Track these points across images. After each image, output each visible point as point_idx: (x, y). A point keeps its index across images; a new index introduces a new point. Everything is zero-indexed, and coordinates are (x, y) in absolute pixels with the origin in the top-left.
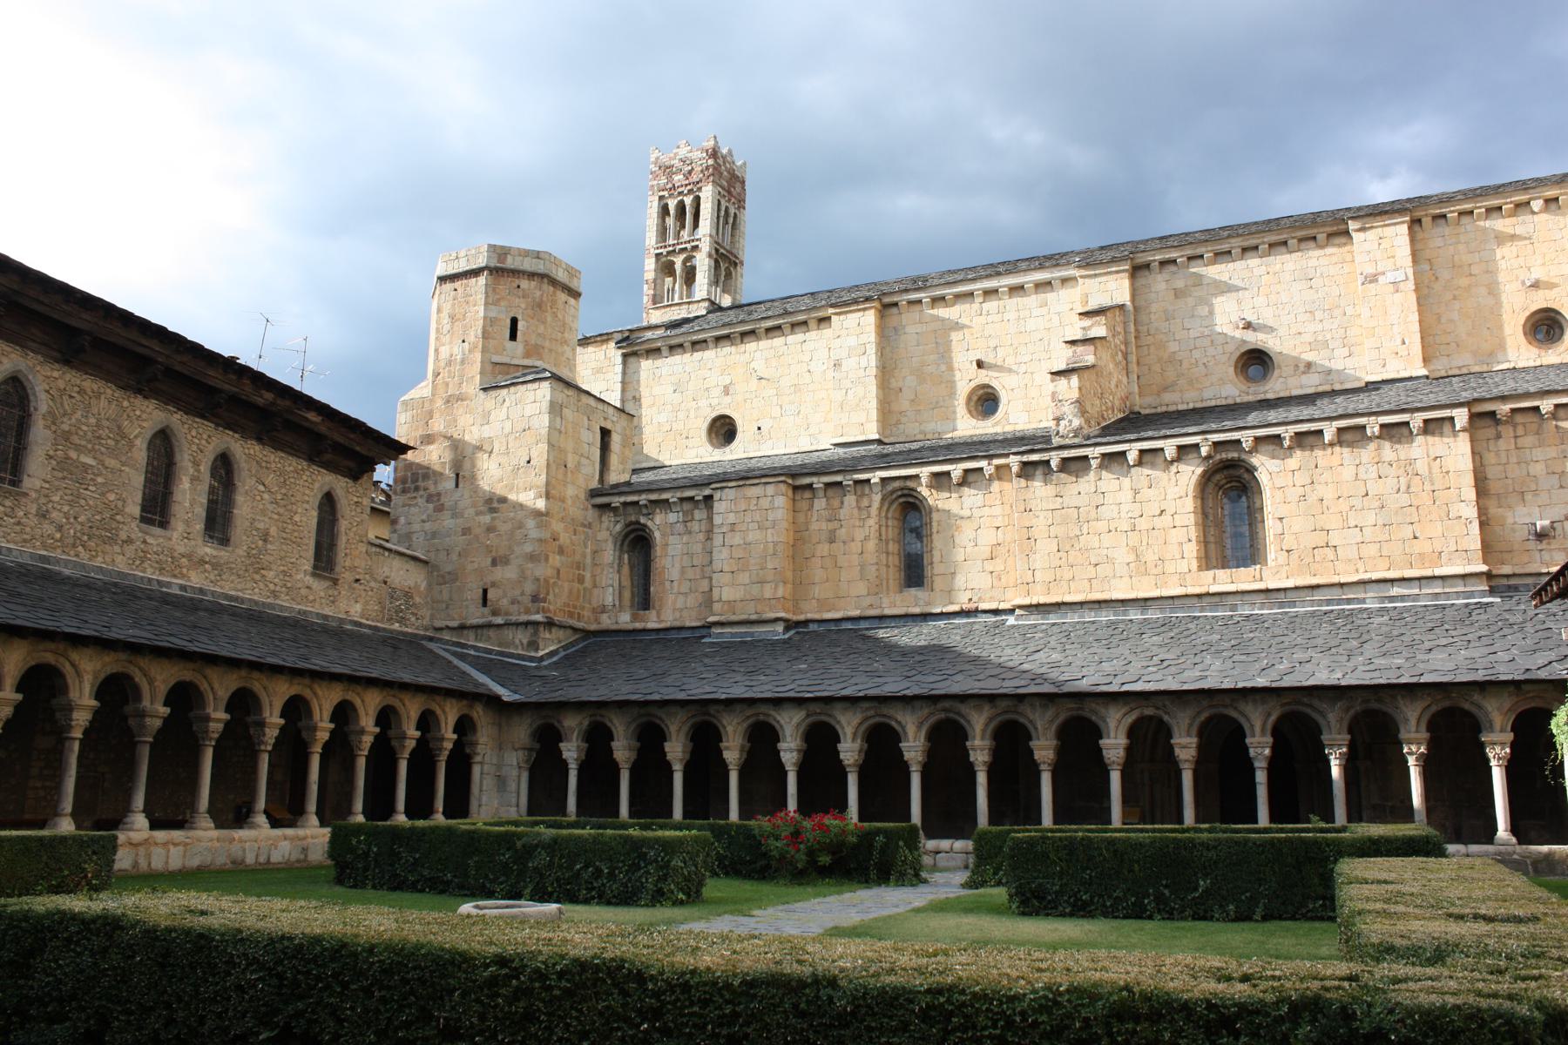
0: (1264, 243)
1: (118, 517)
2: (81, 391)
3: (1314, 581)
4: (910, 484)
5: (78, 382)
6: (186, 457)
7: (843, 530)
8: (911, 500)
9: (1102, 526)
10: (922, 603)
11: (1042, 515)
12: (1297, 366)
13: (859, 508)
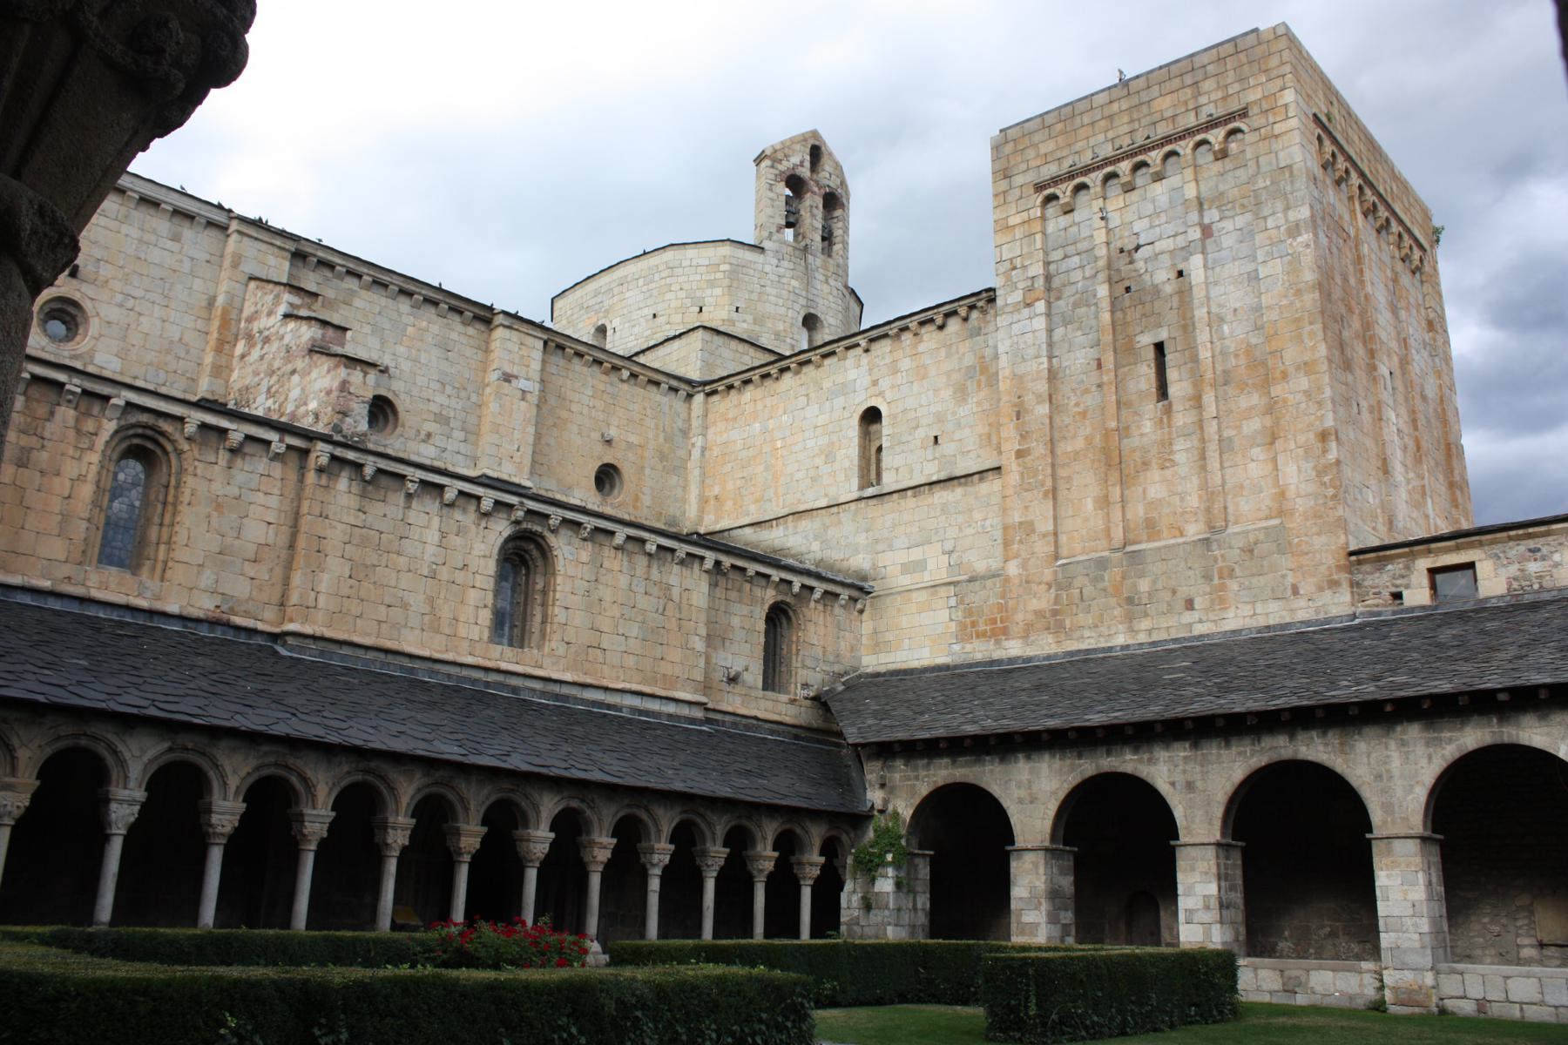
0: (419, 294)
3: (589, 680)
4: (166, 426)
7: (44, 455)
8: (150, 445)
9: (402, 561)
10: (148, 594)
11: (340, 527)
12: (418, 431)
13: (78, 431)
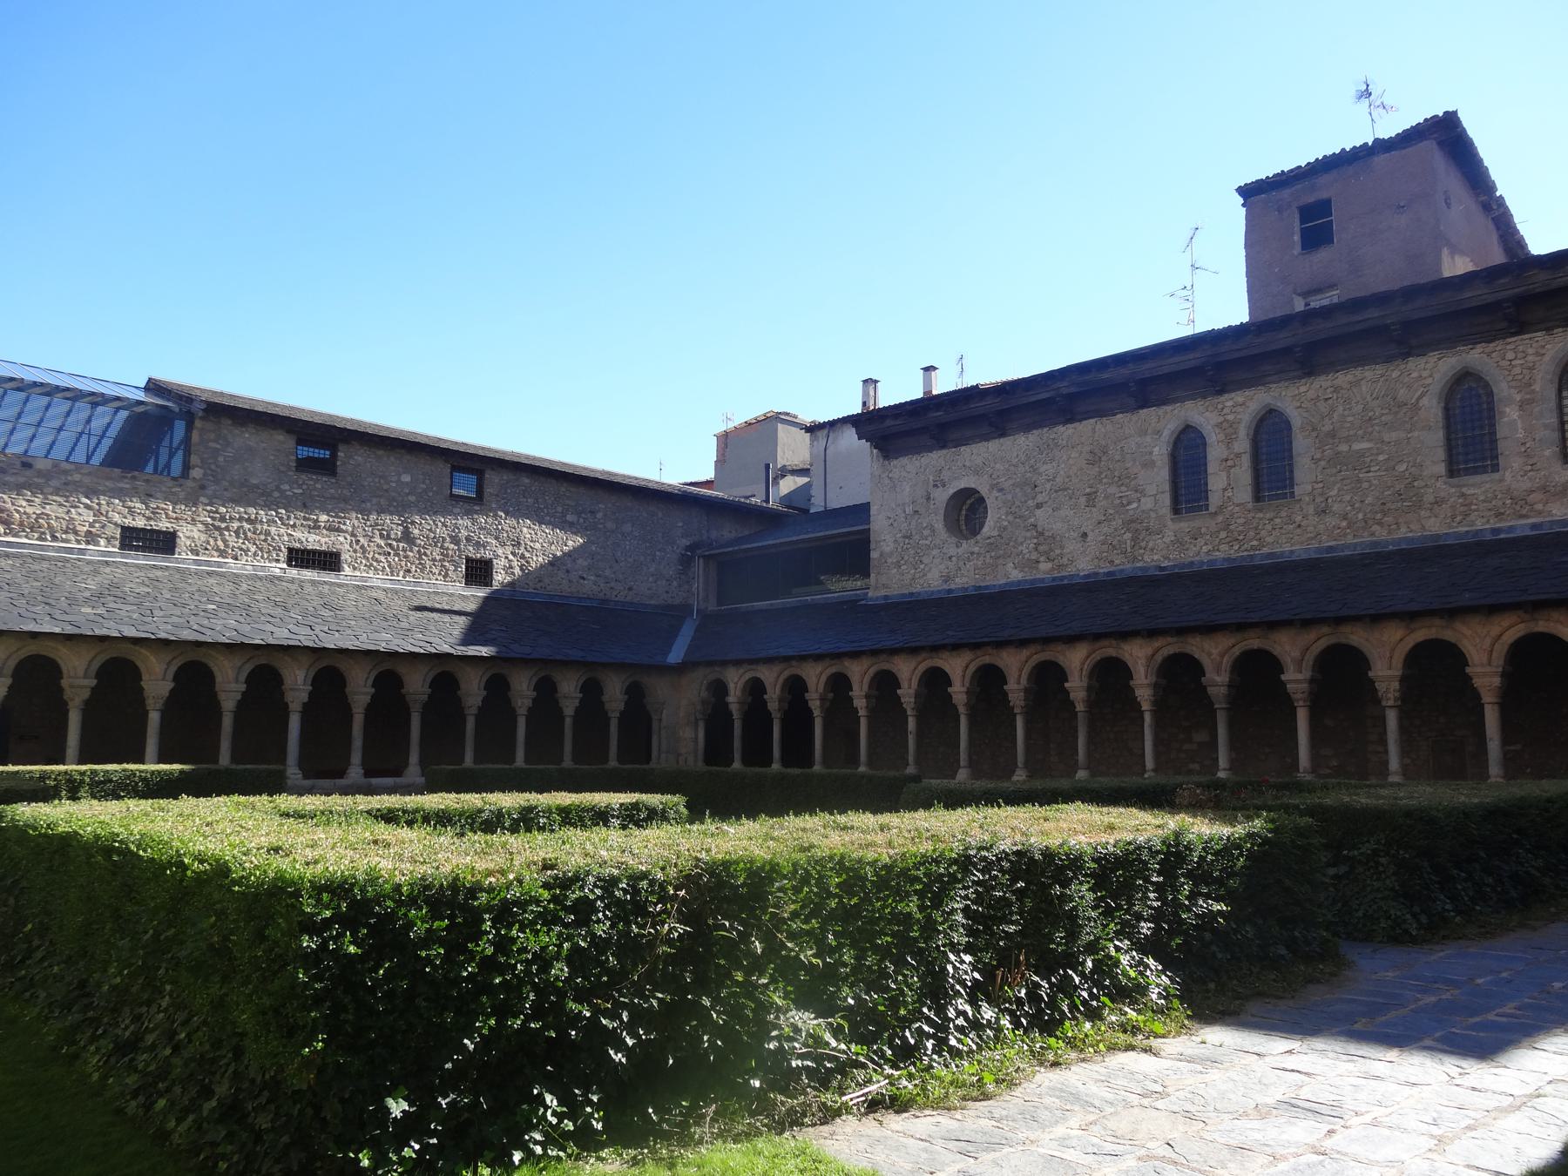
1: (1416, 484)
2: (1336, 389)
5: (1329, 383)
6: (1504, 385)
